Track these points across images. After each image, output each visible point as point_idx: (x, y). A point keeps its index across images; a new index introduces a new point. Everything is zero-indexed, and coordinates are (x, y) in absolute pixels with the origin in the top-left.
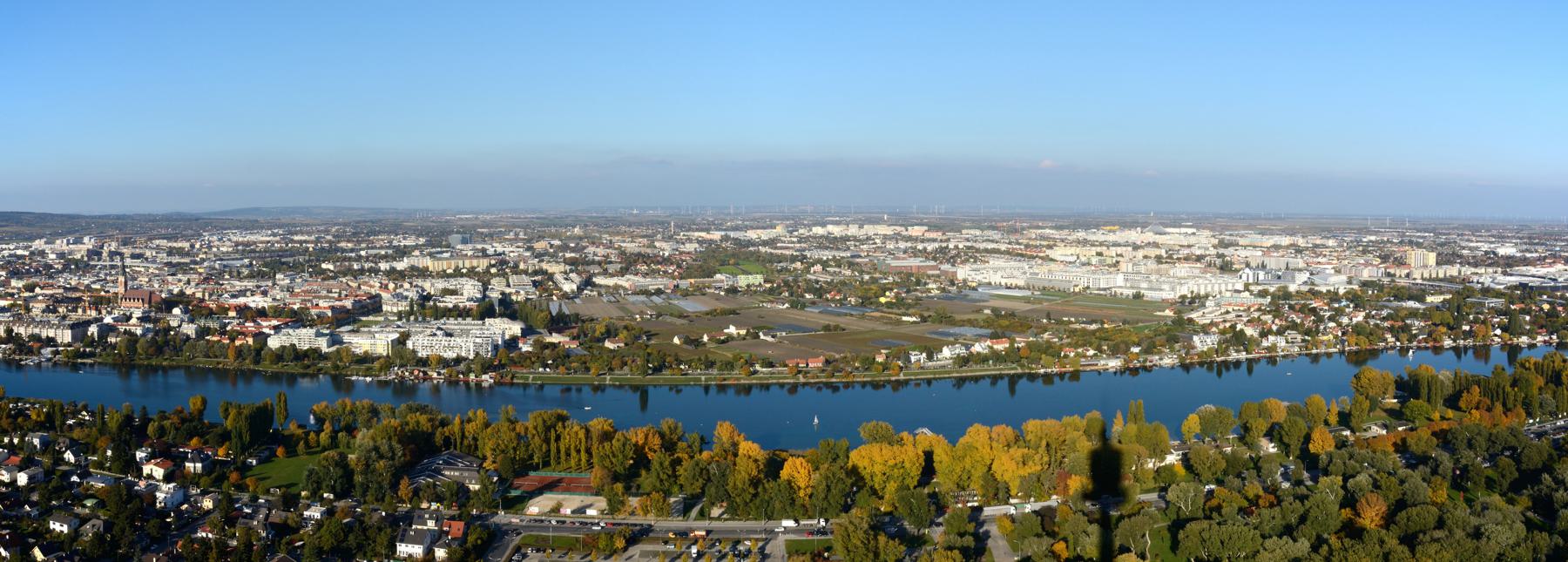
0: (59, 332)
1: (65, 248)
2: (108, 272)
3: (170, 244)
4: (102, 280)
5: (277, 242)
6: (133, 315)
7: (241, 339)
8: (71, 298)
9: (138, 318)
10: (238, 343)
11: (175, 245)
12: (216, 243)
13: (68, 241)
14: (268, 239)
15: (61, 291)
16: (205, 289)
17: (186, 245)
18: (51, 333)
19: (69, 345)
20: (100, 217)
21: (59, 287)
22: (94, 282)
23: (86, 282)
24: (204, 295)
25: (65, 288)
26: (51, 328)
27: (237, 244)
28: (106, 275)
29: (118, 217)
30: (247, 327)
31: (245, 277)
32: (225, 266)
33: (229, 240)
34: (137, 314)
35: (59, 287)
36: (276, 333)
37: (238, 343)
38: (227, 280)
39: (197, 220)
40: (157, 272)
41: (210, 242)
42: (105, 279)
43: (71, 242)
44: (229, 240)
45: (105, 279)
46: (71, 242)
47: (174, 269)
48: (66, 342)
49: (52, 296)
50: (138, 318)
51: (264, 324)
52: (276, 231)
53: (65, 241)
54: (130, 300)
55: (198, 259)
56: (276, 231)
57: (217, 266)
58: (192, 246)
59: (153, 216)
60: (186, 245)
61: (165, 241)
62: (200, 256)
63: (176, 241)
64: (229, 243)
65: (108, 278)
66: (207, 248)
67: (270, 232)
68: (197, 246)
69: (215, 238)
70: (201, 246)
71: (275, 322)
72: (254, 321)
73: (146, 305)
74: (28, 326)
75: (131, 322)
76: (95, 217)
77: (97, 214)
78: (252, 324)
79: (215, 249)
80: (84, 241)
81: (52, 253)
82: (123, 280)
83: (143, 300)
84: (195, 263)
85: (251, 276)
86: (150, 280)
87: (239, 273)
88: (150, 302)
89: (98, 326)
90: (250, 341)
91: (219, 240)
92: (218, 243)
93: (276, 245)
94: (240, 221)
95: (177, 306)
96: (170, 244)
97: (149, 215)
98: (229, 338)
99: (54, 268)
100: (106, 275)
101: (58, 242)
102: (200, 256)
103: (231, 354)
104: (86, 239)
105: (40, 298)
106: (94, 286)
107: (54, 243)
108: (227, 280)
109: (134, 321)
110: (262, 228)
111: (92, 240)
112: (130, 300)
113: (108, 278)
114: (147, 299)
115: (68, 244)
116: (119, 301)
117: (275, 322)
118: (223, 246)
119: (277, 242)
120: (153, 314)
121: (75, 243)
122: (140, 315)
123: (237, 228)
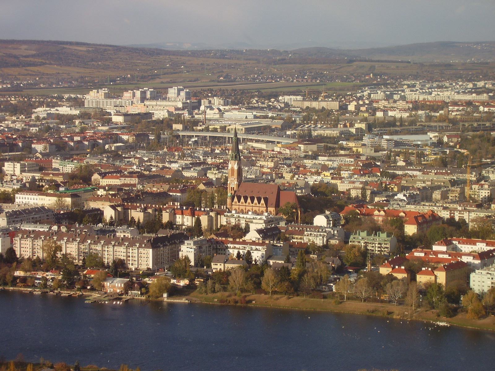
0: (133, 252)
1: (138, 108)
2: (208, 149)
3: (307, 104)
4: (199, 164)
5: (483, 104)
6: (253, 227)
7: (426, 273)
8: (151, 194)
9: (259, 231)
10: (422, 279)
11: (315, 105)
12: (382, 104)
13: (143, 93)
14: (468, 97)
15: (134, 181)
16: (366, 183)
17: (334, 105)
18: (121, 252)
19: (149, 273)
20: (194, 54)
21: (132, 174)
22: (187, 168)
23: (174, 166)
24: (364, 195)
25: (140, 176)
26: (120, 245)
27: (417, 106)
28: (206, 154)
29: (223, 54)
30: (436, 253)
31: (431, 166)
32: (398, 144)
33: (403, 98)
34: (258, 224)
35: (132, 174)
36: (483, 266)
37: (422, 279)
38: (401, 168)
39: (351, 61)
40: (288, 151)
41: (372, 102)
42: (204, 163)
43: (148, 96)
44: (403, 98)
45: (204, 163)
46: (148, 96)
47: (314, 147)
48: (144, 267)
49: (119, 189)
50: (259, 231)
51: (466, 248)
52: (481, 84)
53: (138, 93)
54: (246, 199)
55: (353, 130)
56: (481, 84)
57: (384, 144)
58: (343, 108)
59: (280, 53)
60: (334, 105)
61: (299, 98)
62: (357, 126)
63: (316, 99)
64: (401, 104)
65: (209, 160)
66: (367, 111)
67: (470, 85)
68: (351, 107)
69: (380, 95)
70: (358, 107)
71: (481, 247)
72: (448, 243)
73: (272, 209)
74: (83, 241)
75: (248, 237)
76: (184, 53)
77: (187, 46)
78: (444, 248)
79: (380, 114)
80: (169, 95)
81: (118, 113)
82: (236, 167)
83: (266, 200)
84: (348, 137)
85: (444, 163)
86: (276, 167)
87: (421, 155)
88: (277, 205)
89: (195, 243)
90: (441, 277)
91: (388, 98)
92: (385, 103)
93: (481, 108)
94: (422, 65)
95: (322, 212)
96: (307, 104)
97: (274, 52)
98: (408, 270)
99: (122, 141)
100: (206, 154)
101: (127, 95)
102: (357, 126)
103: (412, 298)
104: (172, 92)
105: (101, 192)
106: (186, 174)
107: (119, 96)
108: (401, 168)
109: (252, 236)
110: (456, 77)
111: (183, 94)
112: (246, 199)
113: (209, 160)
114: (272, 199)
115: (143, 99)
116: (229, 201)
117: (481, 247)
118: (393, 109)
119: (483, 104)
120: (282, 224)
121: (154, 97)
122: (262, 226)
123: (416, 77)
